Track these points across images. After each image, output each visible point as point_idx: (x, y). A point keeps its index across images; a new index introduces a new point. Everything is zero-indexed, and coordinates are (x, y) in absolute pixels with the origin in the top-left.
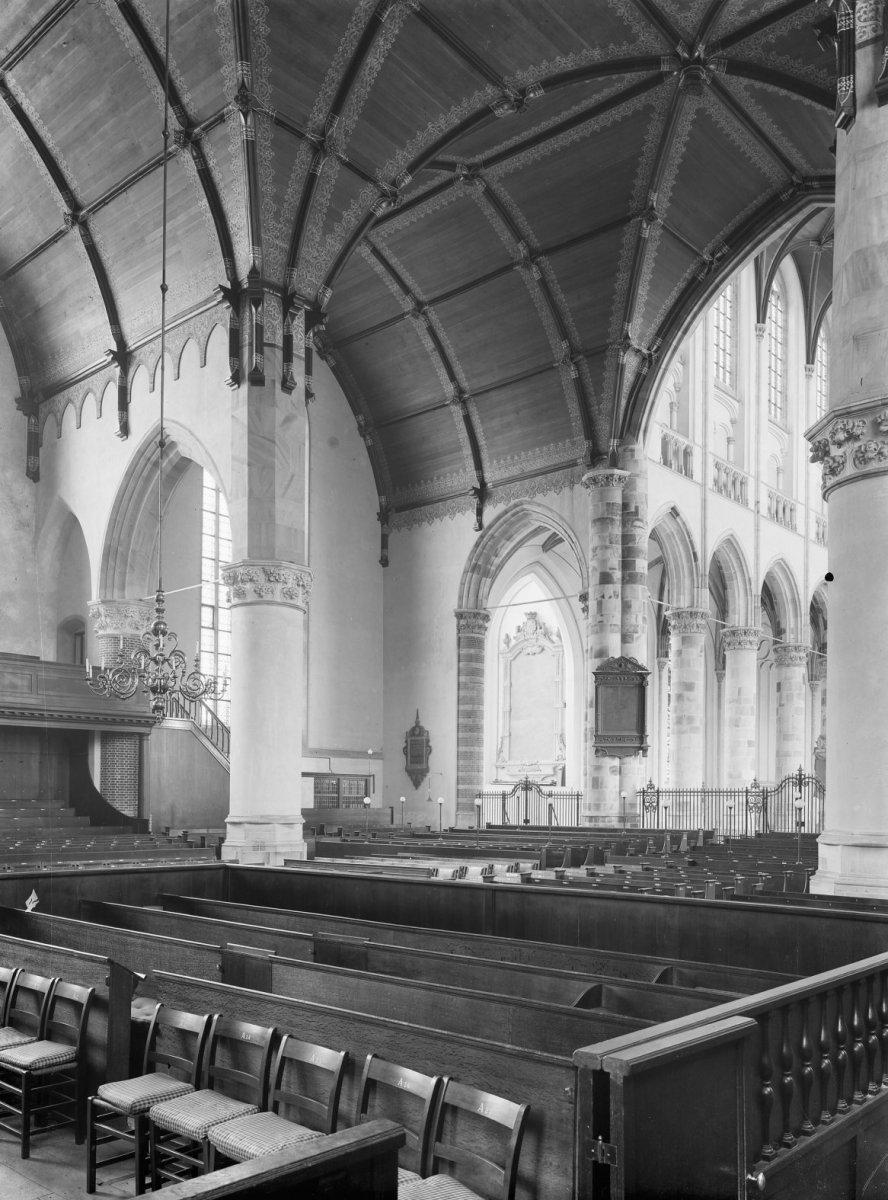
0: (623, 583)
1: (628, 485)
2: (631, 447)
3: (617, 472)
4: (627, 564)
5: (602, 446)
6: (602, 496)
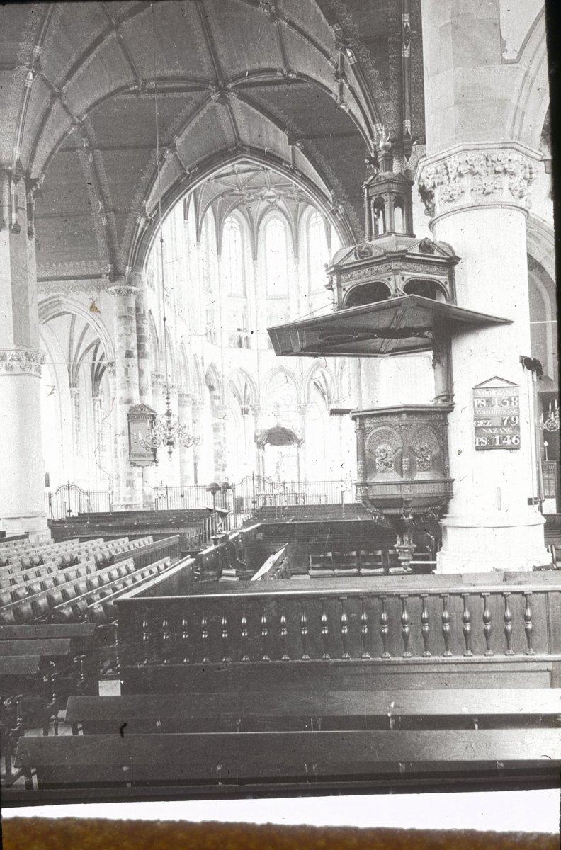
0: (139, 358)
1: (139, 296)
2: (139, 273)
3: (134, 288)
4: (140, 347)
5: (120, 268)
6: (125, 303)
